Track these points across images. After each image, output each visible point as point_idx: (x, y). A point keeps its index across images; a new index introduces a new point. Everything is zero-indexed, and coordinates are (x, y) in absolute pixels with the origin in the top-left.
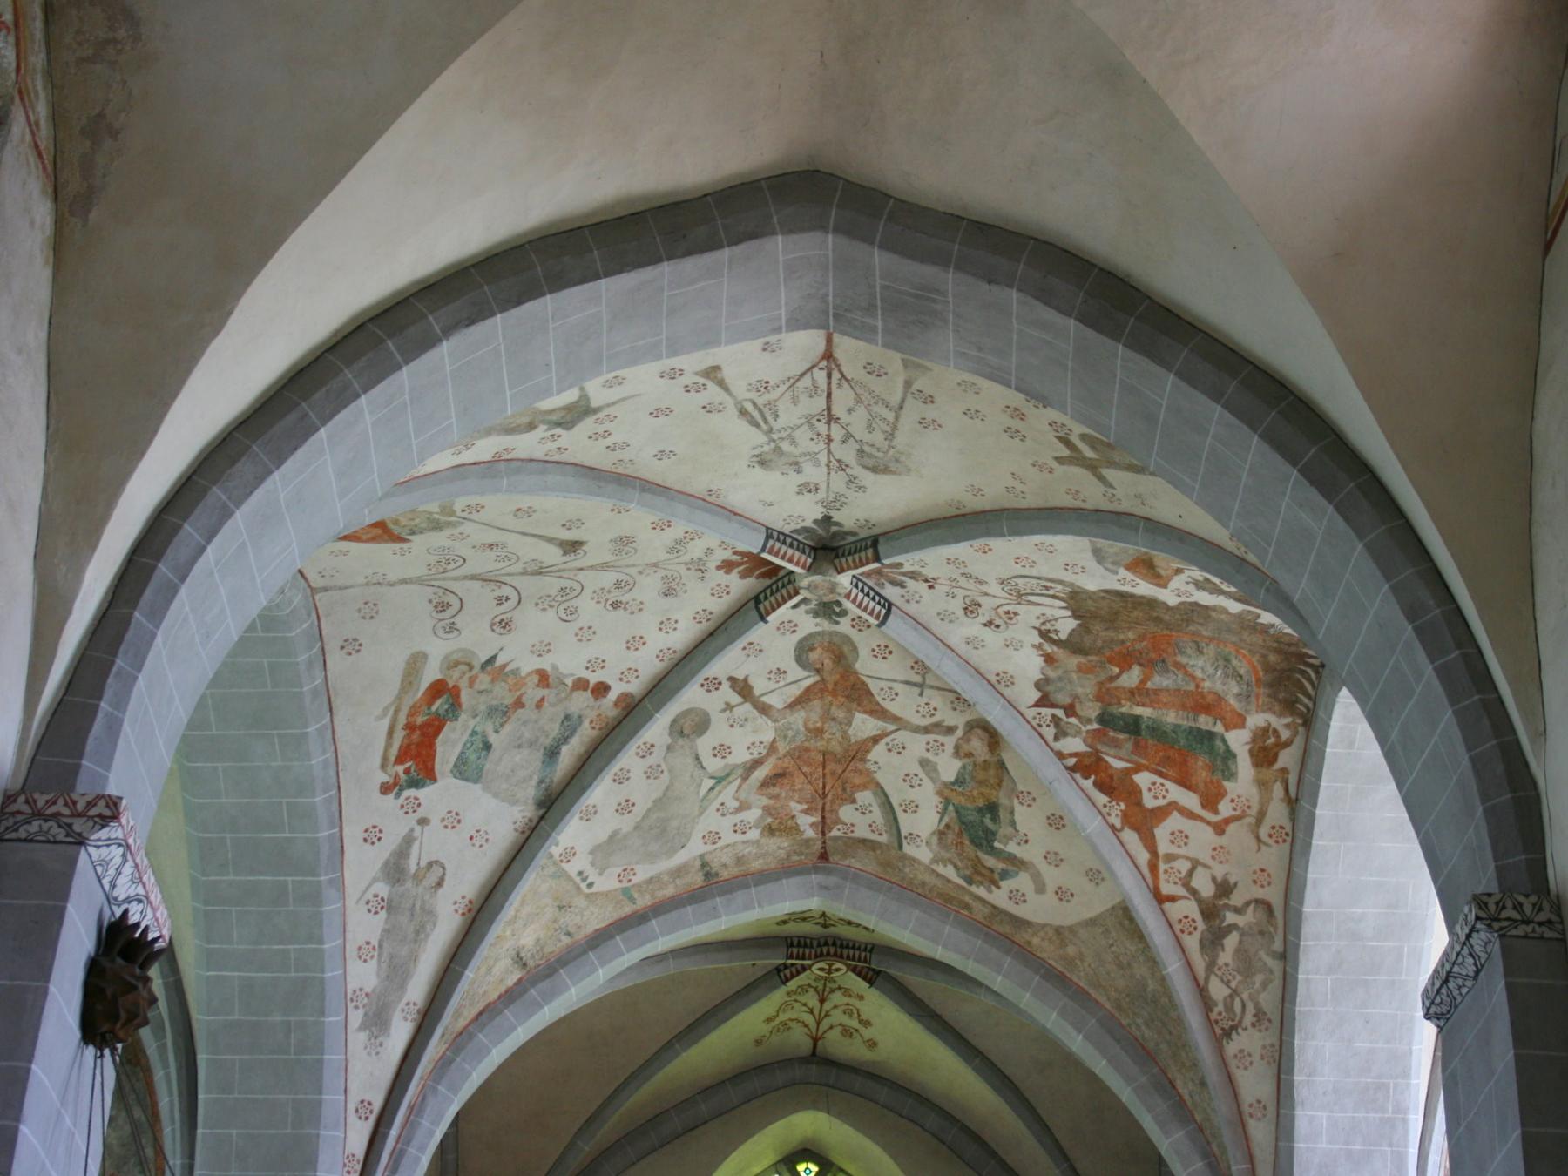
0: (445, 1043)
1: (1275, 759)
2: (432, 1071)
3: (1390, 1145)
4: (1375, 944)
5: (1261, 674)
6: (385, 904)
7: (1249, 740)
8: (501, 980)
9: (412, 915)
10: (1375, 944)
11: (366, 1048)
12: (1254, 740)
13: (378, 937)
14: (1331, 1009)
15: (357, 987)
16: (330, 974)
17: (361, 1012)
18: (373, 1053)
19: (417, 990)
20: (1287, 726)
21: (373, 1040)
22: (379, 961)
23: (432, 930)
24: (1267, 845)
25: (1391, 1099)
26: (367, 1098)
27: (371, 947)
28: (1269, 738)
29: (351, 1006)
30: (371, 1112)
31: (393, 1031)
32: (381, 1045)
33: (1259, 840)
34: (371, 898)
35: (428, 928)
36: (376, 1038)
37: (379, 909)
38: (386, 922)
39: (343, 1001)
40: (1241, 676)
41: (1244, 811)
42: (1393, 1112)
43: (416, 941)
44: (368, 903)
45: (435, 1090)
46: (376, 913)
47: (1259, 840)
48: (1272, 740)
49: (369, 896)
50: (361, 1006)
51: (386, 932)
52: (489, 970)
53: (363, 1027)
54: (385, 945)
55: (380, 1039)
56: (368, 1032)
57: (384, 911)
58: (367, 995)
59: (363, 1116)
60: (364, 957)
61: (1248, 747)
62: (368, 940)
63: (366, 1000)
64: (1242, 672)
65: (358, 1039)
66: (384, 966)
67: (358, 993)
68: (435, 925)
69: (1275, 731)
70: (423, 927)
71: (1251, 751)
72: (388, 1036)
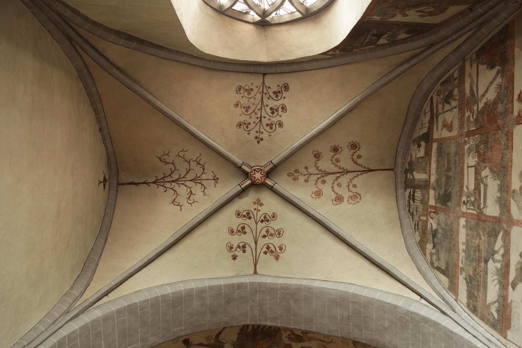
1: (299, 335)
3: (420, 322)
4: (350, 312)
5: (267, 340)
7: (295, 343)
10: (350, 312)
12: (295, 341)
14: (374, 333)
20: (285, 332)
24: (332, 339)
25: (404, 316)
28: (292, 337)
33: (331, 342)
40: (269, 346)
41: (322, 346)
42: (409, 317)
47: (331, 342)
48: (292, 336)
61: (297, 343)
64: (268, 346)
69: (288, 335)
71: (300, 342)
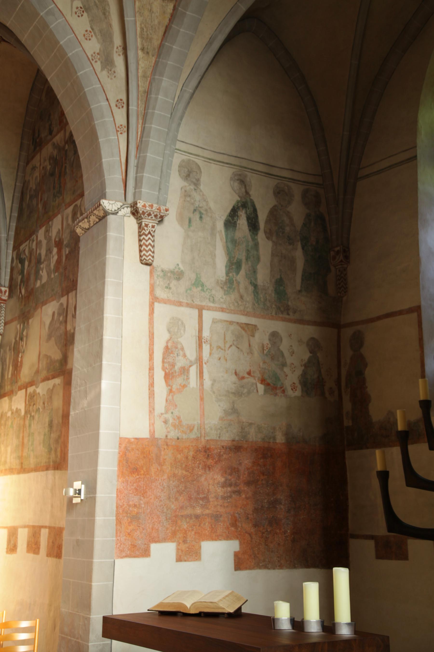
0: (153, 56)
2: (152, 71)
6: (83, 9)
8: (164, 12)
9: (97, 7)
11: (108, 77)
13: (89, 26)
15: (92, 53)
16: (70, 54)
17: (99, 63)
18: (113, 77)
19: (117, 41)
21: (110, 72)
22: (96, 36)
23: (109, 8)
26: (119, 98)
27: (88, 32)
29: (93, 62)
30: (123, 103)
31: (116, 63)
32: (114, 72)
34: (76, 10)
35: (107, 9)
36: (111, 70)
37: (82, 13)
38: (89, 17)
39: (89, 62)
43: (106, 18)
44: (76, 13)
45: (154, 79)
46: (82, 15)
49: (75, 10)
50: (97, 60)
51: (92, 21)
52: (151, 11)
53: (102, 69)
54: (94, 27)
55: (113, 70)
56: (106, 69)
57: (85, 12)
58: (98, 54)
59: (121, 107)
60: (88, 38)
62: (85, 29)
63: (99, 57)
65: (103, 75)
66: (99, 37)
67: (94, 55)
68: (108, 5)
70: (105, 9)
72: (116, 66)
